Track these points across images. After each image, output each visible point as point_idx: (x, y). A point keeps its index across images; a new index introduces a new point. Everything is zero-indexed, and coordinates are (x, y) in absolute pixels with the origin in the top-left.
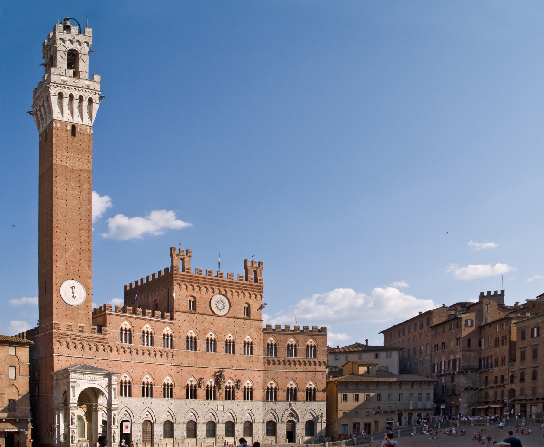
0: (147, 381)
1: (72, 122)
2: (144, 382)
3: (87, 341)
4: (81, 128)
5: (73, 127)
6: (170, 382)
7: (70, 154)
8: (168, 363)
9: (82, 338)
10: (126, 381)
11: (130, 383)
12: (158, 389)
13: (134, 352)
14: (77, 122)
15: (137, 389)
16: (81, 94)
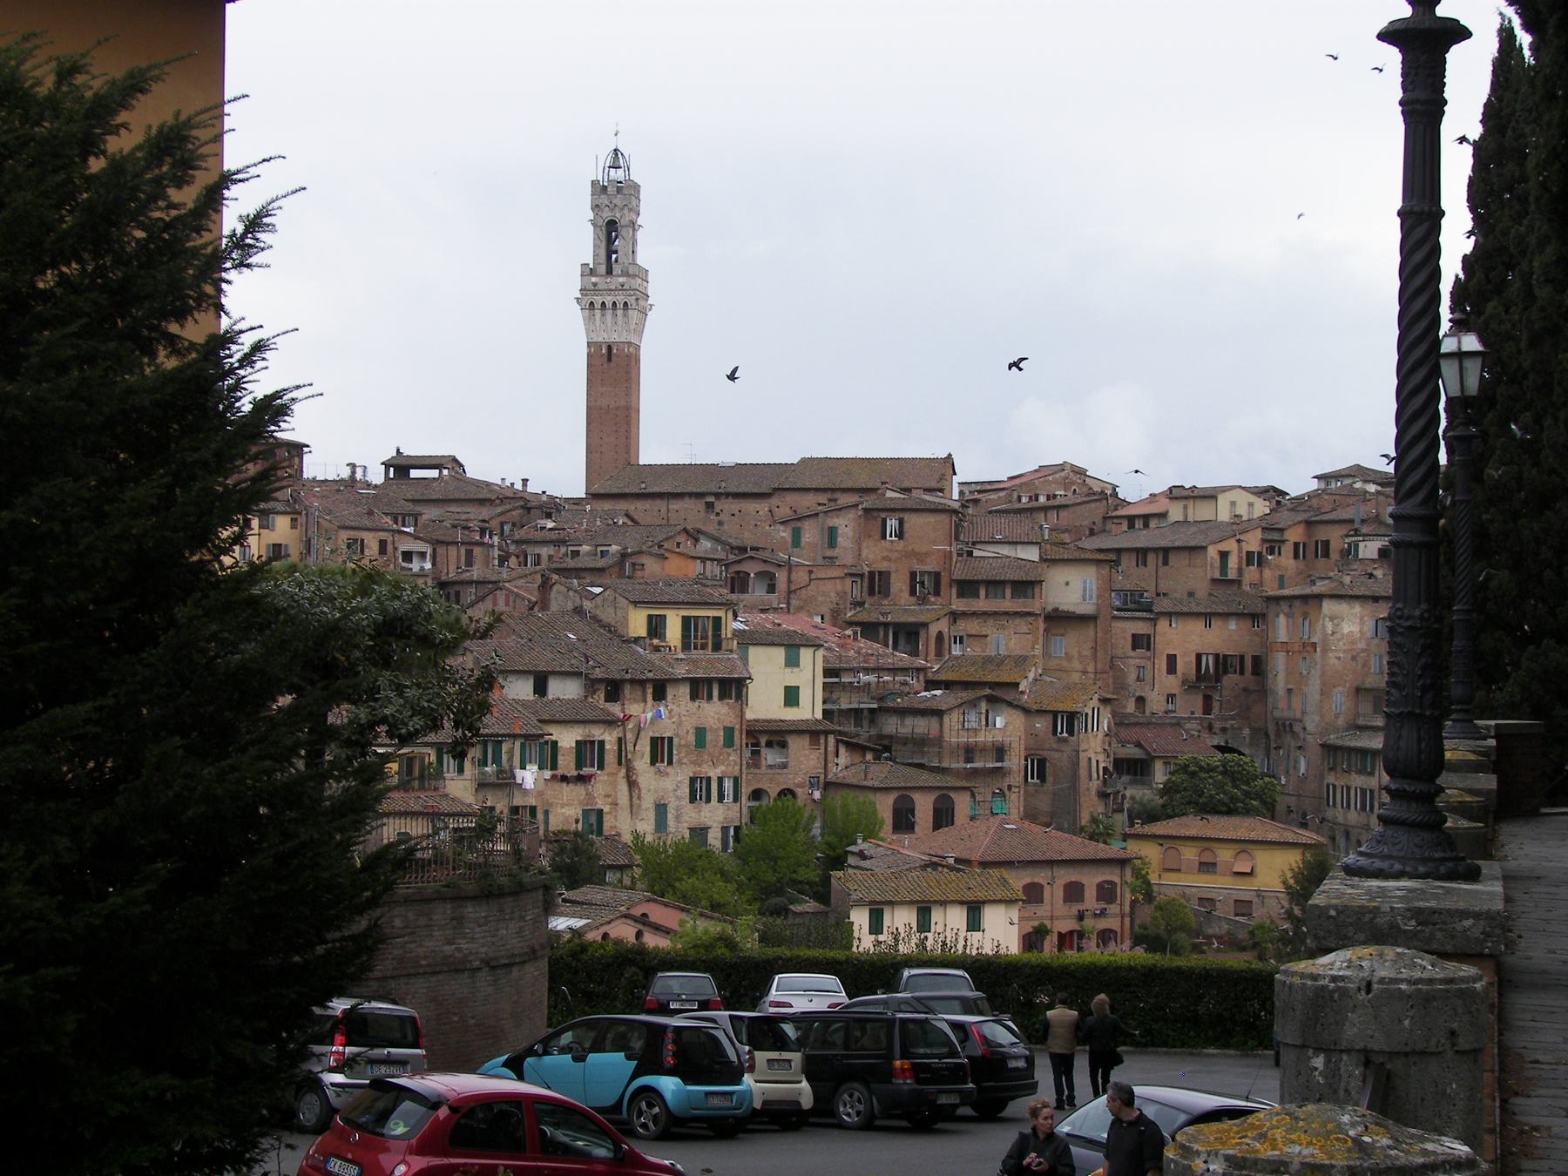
5: (610, 348)
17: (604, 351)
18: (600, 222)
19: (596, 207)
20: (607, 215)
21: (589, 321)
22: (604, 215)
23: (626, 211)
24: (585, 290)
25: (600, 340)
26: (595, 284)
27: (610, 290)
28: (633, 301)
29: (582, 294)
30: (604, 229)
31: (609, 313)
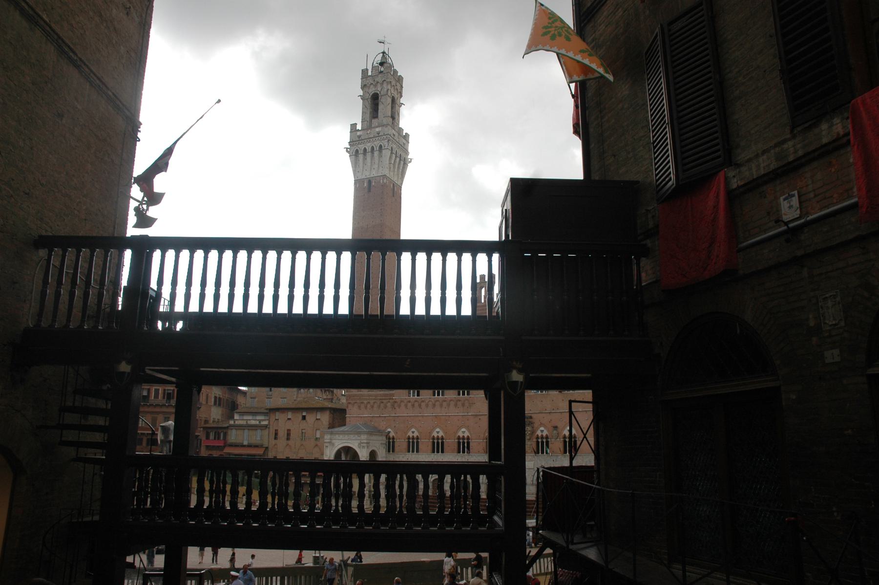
0: (437, 435)
1: (369, 177)
2: (434, 436)
3: (374, 399)
4: (376, 181)
5: (370, 182)
6: (466, 434)
7: (365, 213)
8: (463, 413)
9: (371, 397)
10: (413, 436)
11: (418, 438)
12: (451, 443)
13: (423, 404)
14: (372, 176)
15: (426, 444)
16: (373, 145)
17: (365, 185)
18: (368, 96)
19: (364, 87)
20: (372, 90)
21: (355, 165)
22: (370, 91)
23: (385, 85)
24: (353, 141)
25: (364, 177)
26: (359, 137)
27: (371, 138)
28: (386, 144)
29: (350, 145)
30: (369, 100)
31: (369, 155)
